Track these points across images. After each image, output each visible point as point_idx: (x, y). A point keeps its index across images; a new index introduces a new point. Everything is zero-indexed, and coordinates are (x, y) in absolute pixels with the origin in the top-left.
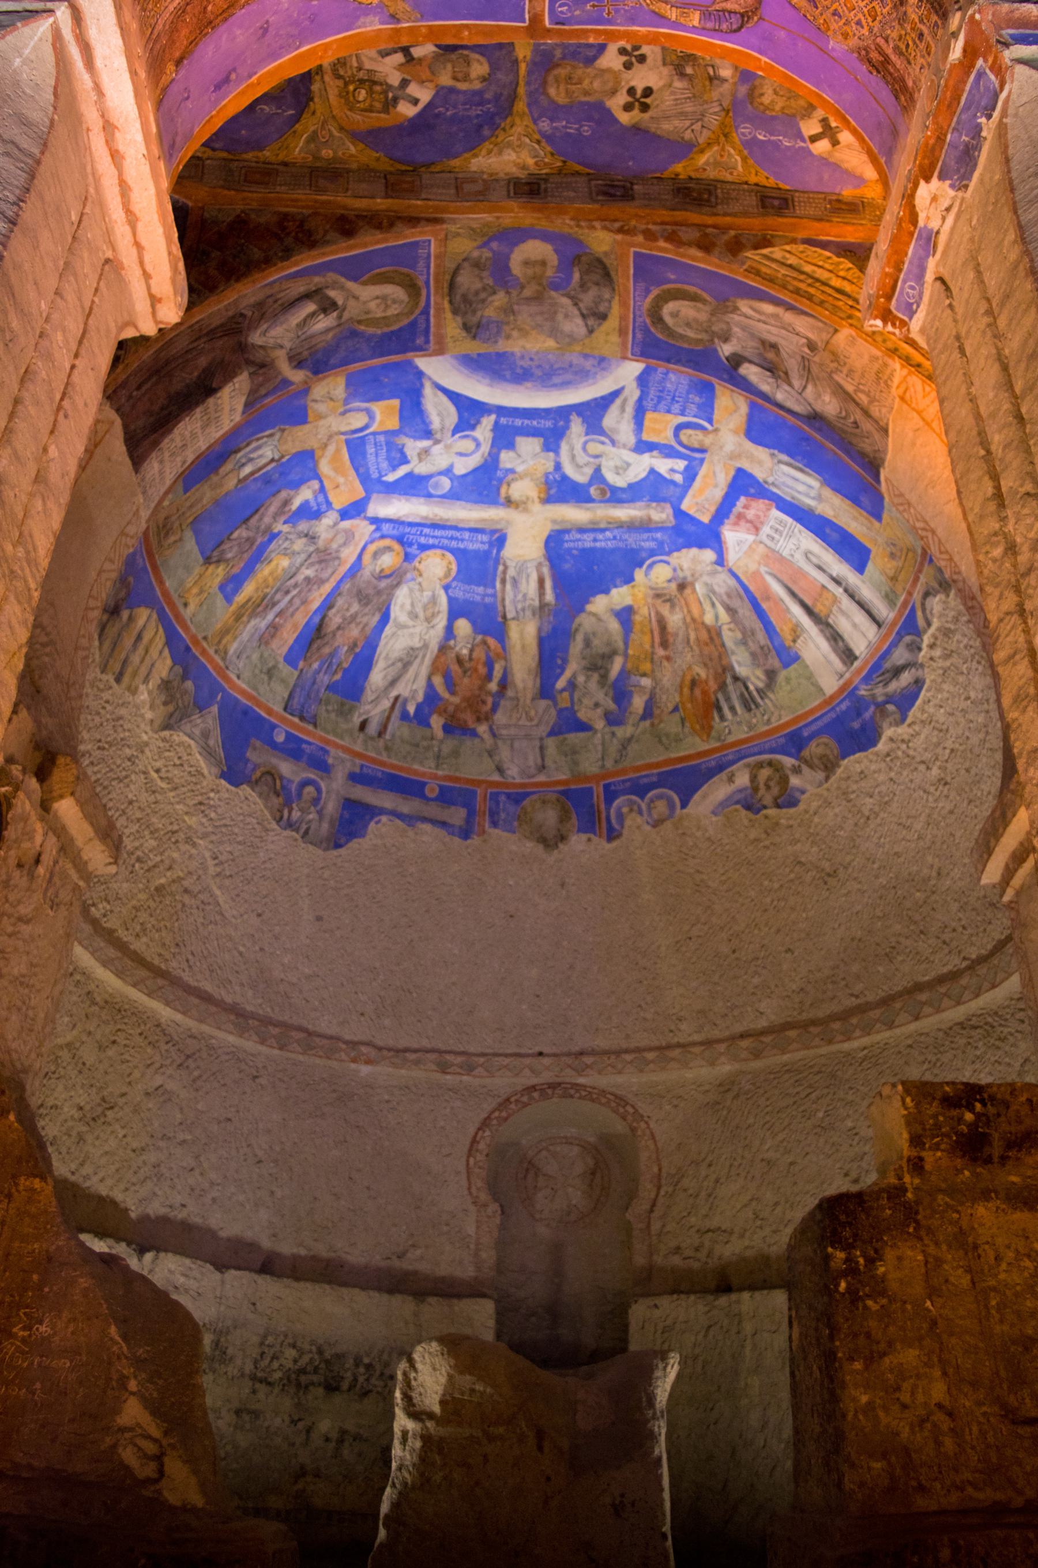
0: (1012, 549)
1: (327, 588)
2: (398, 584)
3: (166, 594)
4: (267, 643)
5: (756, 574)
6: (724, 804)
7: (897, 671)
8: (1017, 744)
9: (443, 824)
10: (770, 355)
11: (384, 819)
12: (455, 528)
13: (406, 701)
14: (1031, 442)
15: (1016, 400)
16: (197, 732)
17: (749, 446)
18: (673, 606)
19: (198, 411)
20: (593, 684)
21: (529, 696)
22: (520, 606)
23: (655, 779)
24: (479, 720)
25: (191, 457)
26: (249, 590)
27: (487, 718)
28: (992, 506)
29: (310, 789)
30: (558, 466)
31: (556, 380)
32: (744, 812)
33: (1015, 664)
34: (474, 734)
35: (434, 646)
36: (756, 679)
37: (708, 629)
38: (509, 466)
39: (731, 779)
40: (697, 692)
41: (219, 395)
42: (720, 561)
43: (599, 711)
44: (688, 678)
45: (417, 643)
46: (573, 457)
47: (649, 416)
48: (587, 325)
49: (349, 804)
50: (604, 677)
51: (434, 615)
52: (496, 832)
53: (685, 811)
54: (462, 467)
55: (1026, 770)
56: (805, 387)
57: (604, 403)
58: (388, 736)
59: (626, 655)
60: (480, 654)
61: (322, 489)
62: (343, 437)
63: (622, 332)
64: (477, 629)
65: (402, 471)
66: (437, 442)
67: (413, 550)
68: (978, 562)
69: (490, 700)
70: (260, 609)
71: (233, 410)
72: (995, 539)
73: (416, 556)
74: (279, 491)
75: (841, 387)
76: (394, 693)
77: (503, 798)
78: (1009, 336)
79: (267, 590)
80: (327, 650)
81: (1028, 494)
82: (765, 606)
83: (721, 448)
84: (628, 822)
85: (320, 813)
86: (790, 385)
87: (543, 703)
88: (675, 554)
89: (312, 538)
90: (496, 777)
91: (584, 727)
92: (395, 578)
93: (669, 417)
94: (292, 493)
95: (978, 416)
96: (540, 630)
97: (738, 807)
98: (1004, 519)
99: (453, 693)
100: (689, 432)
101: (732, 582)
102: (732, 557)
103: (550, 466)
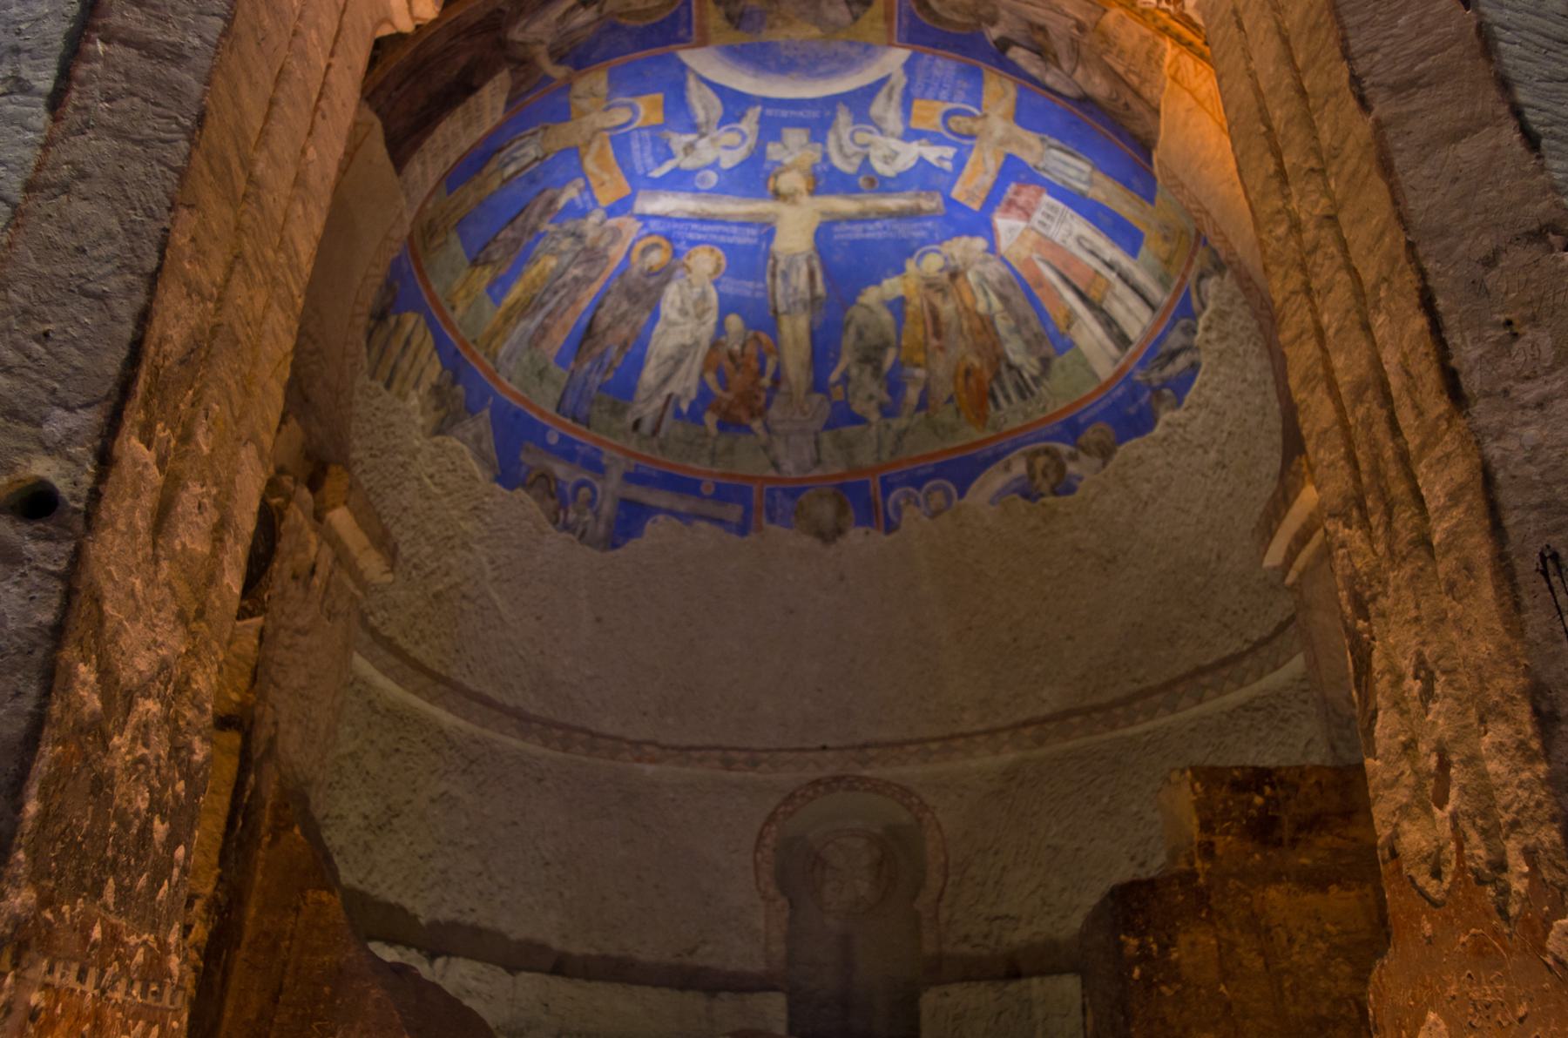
0: (1296, 227)
1: (596, 287)
2: (667, 282)
3: (433, 298)
4: (537, 345)
5: (1028, 262)
6: (1001, 493)
7: (1173, 355)
8: (1306, 426)
9: (720, 522)
10: (1039, 38)
11: (661, 518)
12: (724, 222)
13: (678, 399)
14: (1315, 117)
15: (1297, 74)
16: (469, 436)
17: (1018, 131)
18: (945, 296)
19: (459, 111)
20: (867, 377)
22: (791, 300)
23: (931, 470)
24: (752, 416)
25: (453, 158)
26: (517, 291)
27: (759, 413)
28: (1275, 184)
29: (584, 491)
30: (826, 157)
31: (822, 69)
32: (1021, 502)
33: (1302, 344)
34: (748, 430)
35: (705, 343)
36: (1029, 366)
37: (981, 318)
38: (776, 158)
39: (1007, 468)
40: (972, 382)
41: (479, 93)
42: (992, 248)
43: (874, 404)
44: (962, 368)
45: (687, 340)
46: (841, 148)
47: (917, 104)
48: (851, 12)
49: (626, 504)
50: (877, 370)
51: (704, 312)
52: (774, 528)
53: (964, 501)
54: (729, 160)
55: (1316, 453)
56: (1074, 70)
57: (870, 92)
58: (662, 434)
59: (899, 346)
60: (751, 349)
61: (588, 187)
62: (607, 134)
63: (888, 18)
64: (748, 324)
65: (668, 166)
66: (702, 136)
67: (682, 246)
68: (1261, 242)
69: (763, 396)
70: (529, 310)
71: (494, 109)
72: (1279, 217)
73: (683, 253)
74: (543, 191)
75: (1111, 68)
76: (666, 391)
77: (778, 494)
78: (1290, 8)
79: (535, 291)
80: (597, 350)
81: (1312, 170)
82: (1038, 292)
83: (990, 133)
84: (906, 514)
85: (596, 514)
86: (1059, 66)
88: (947, 243)
89: (578, 236)
90: (771, 473)
91: (858, 420)
92: (665, 274)
93: (937, 104)
94: (557, 191)
95: (1258, 92)
96: (811, 324)
97: (1016, 496)
98: (1287, 197)
99: (726, 389)
100: (958, 118)
101: (1004, 270)
102: (1004, 244)
103: (817, 157)
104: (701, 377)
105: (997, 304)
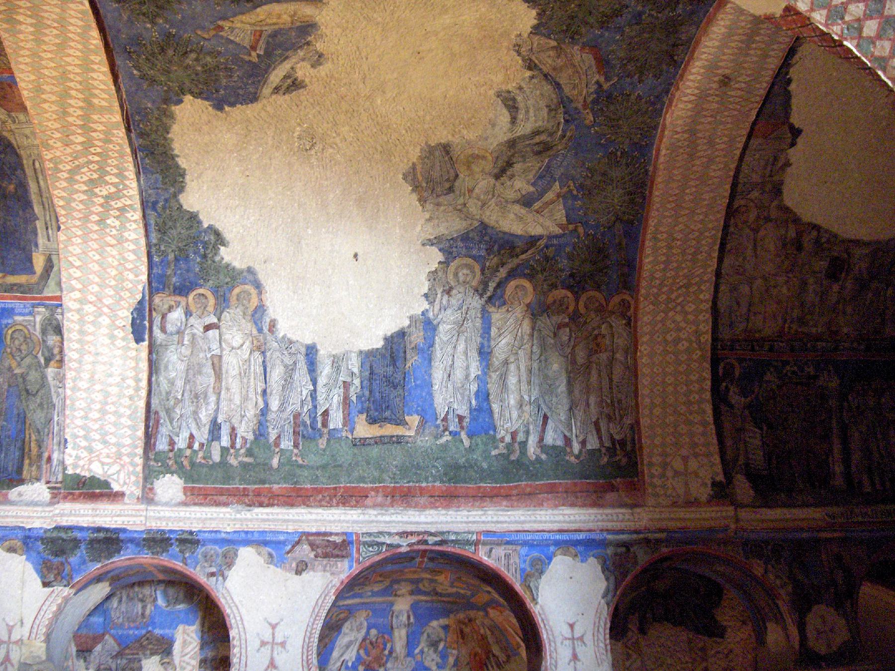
20: (431, 651)
21: (402, 655)
24: (380, 666)
27: (384, 665)
35: (360, 639)
36: (502, 657)
43: (434, 663)
45: (353, 638)
69: (385, 658)
76: (342, 659)
87: (409, 659)
104: (358, 651)
105: (488, 633)
